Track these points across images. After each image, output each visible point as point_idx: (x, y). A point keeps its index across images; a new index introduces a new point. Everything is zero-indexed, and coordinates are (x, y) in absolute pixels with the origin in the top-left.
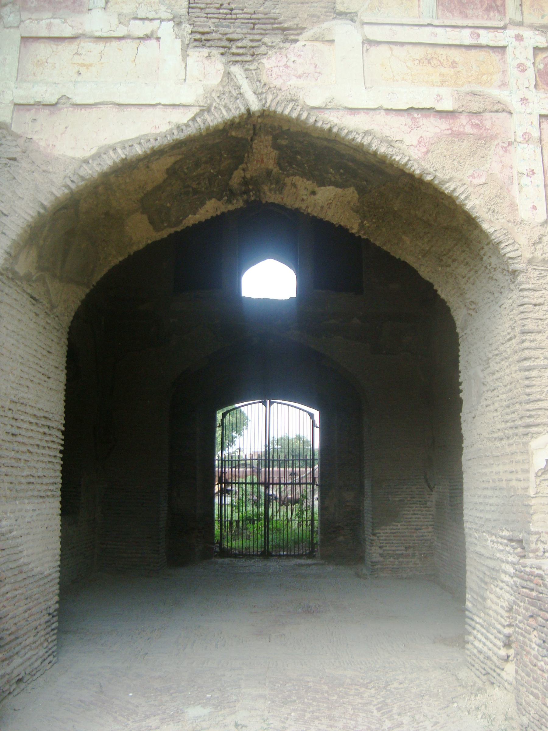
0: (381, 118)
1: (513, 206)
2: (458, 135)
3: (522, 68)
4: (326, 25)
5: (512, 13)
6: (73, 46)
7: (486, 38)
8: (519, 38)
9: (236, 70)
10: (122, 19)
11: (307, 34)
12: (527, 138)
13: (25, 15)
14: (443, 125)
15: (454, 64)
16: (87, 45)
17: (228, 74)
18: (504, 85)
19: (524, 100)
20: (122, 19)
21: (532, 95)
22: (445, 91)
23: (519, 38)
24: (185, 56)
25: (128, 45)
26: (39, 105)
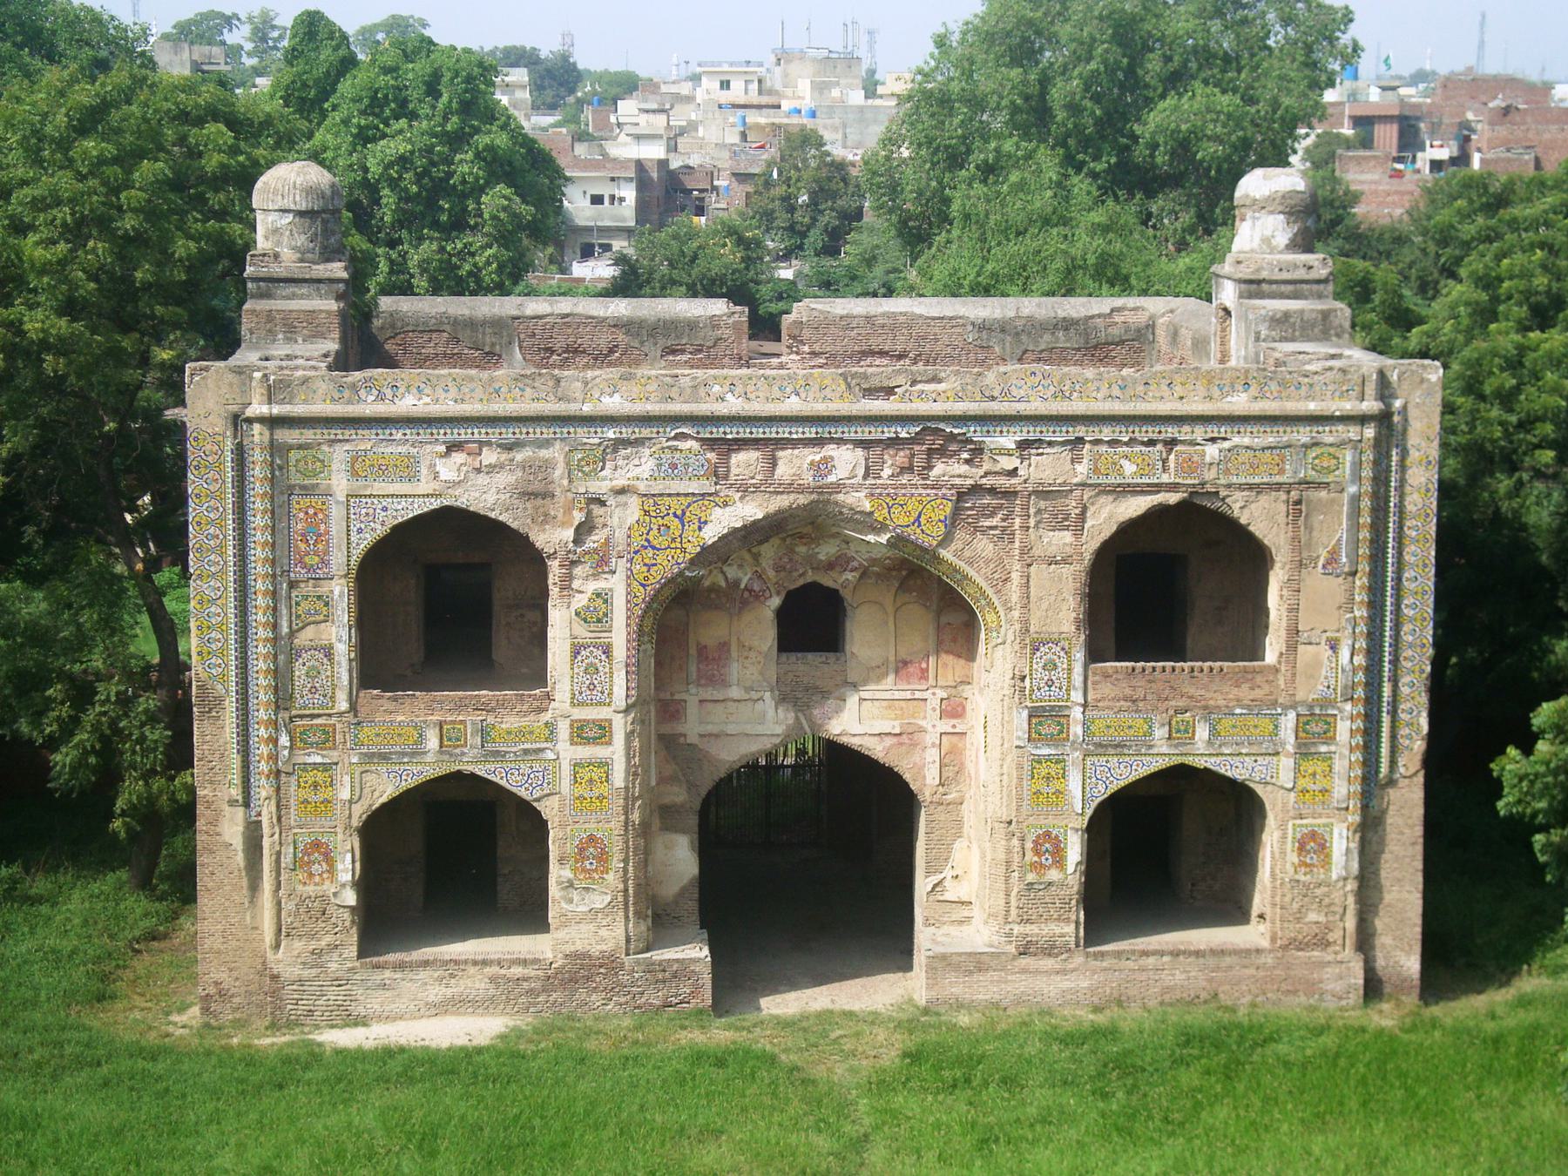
0: (866, 738)
1: (924, 777)
2: (901, 744)
3: (934, 710)
4: (843, 690)
5: (932, 681)
6: (723, 704)
7: (918, 695)
8: (934, 694)
9: (800, 715)
10: (748, 689)
11: (837, 694)
12: (933, 745)
13: (700, 689)
14: (895, 740)
15: (902, 709)
16: (731, 703)
17: (797, 718)
18: (925, 718)
19: (934, 726)
20: (748, 689)
21: (938, 723)
22: (896, 723)
23: (934, 694)
24: (776, 709)
25: (750, 704)
26: (710, 735)
